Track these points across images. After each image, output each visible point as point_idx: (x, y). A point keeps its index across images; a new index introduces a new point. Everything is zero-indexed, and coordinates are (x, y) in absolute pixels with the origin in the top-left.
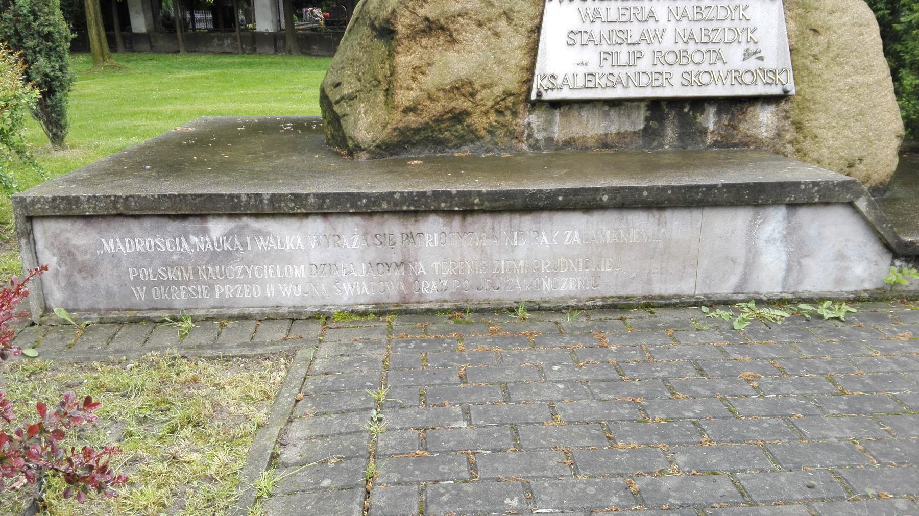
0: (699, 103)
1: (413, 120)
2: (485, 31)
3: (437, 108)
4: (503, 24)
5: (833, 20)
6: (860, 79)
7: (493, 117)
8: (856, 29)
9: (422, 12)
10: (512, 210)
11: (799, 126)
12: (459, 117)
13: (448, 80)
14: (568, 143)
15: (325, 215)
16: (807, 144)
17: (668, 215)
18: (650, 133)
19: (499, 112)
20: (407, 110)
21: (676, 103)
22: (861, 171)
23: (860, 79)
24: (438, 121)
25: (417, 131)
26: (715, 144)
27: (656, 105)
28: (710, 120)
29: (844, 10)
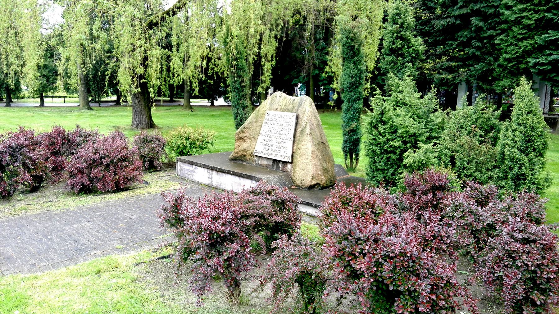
0: (279, 161)
1: (237, 155)
2: (250, 140)
3: (240, 153)
4: (253, 139)
5: (303, 147)
6: (305, 161)
7: (250, 157)
8: (306, 150)
9: (240, 135)
10: (221, 172)
11: (294, 169)
12: (245, 156)
13: (242, 149)
14: (261, 165)
15: (208, 169)
16: (295, 174)
17: (241, 178)
18: (273, 166)
19: (251, 156)
20: (236, 153)
21: (276, 160)
22: (303, 182)
23: (305, 161)
24: (241, 156)
25: (237, 157)
26: (281, 170)
27: (274, 161)
28: (280, 165)
29: (305, 145)
